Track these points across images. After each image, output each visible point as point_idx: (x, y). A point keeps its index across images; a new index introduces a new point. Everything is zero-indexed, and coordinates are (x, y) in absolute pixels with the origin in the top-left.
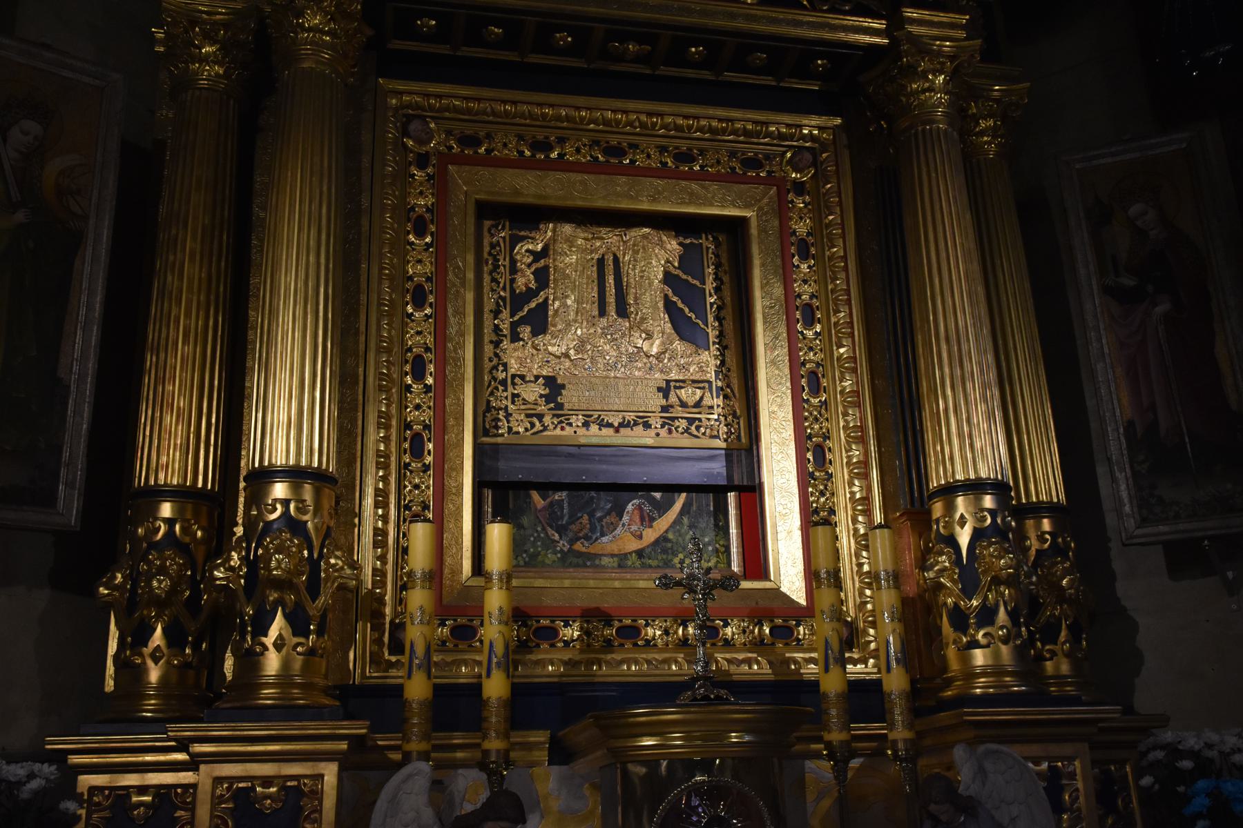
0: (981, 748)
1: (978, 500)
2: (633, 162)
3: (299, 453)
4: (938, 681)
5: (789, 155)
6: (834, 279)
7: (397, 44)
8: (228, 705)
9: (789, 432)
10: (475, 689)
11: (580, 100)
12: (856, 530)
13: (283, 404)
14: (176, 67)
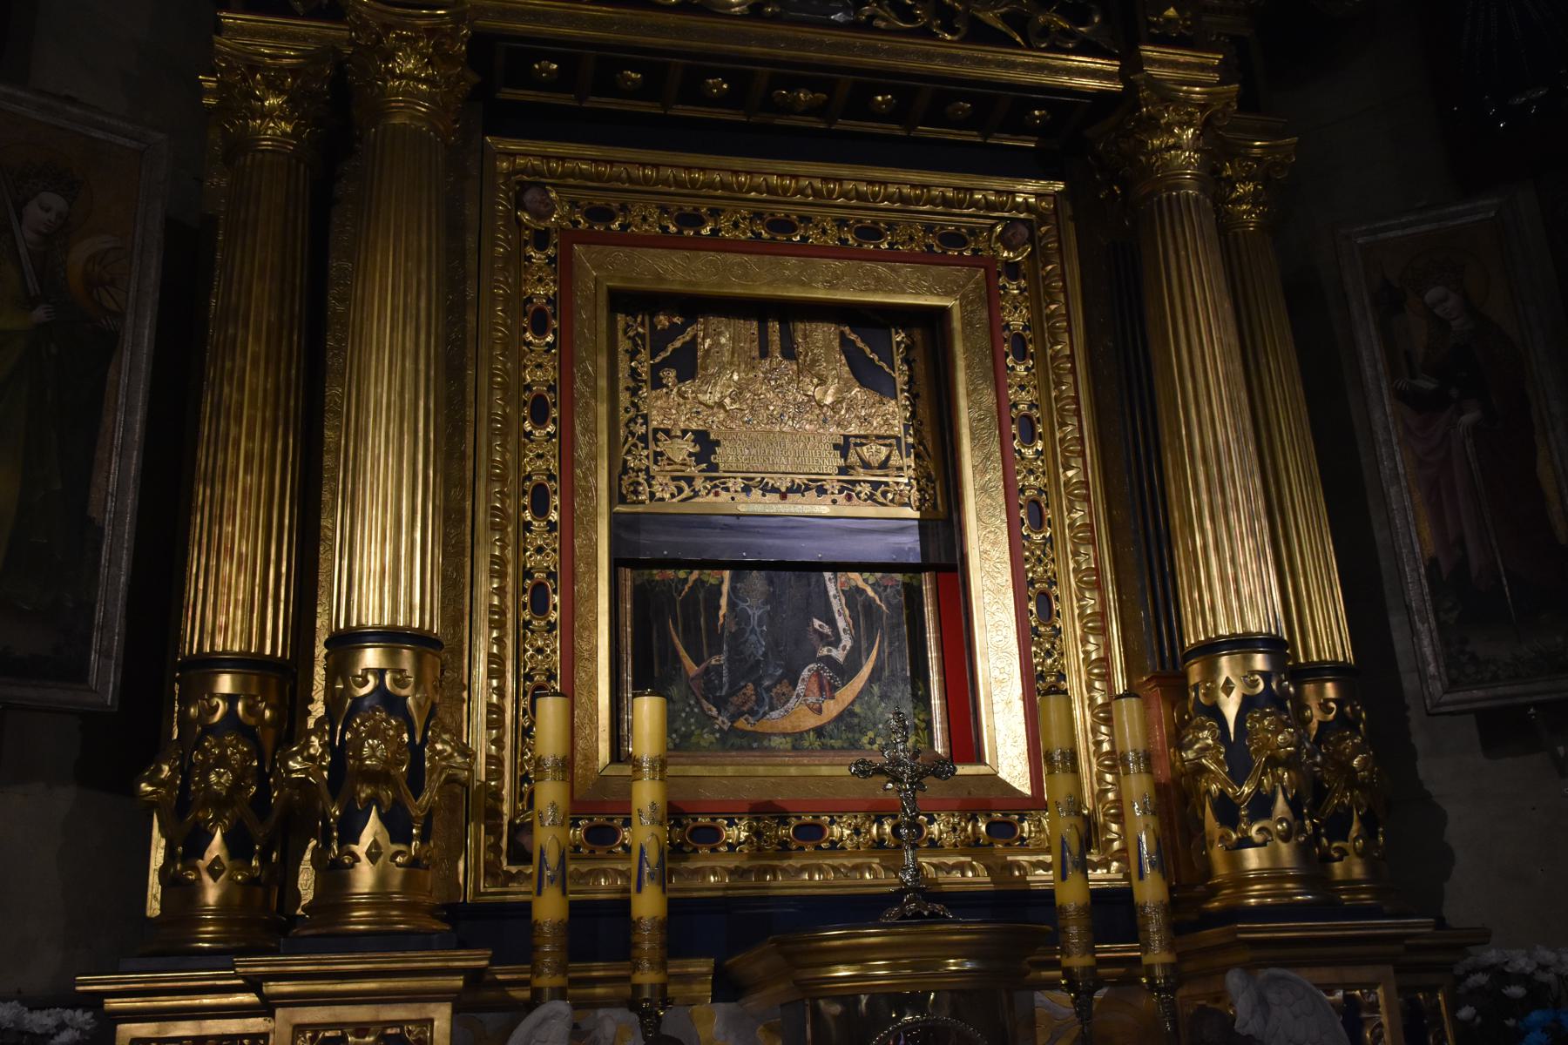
0: (1263, 974)
1: (1247, 660)
2: (804, 239)
3: (395, 610)
4: (1200, 888)
5: (999, 229)
6: (1058, 384)
7: (508, 94)
8: (313, 932)
9: (1005, 577)
10: (621, 907)
11: (738, 163)
12: (1092, 699)
13: (375, 548)
14: (232, 124)
